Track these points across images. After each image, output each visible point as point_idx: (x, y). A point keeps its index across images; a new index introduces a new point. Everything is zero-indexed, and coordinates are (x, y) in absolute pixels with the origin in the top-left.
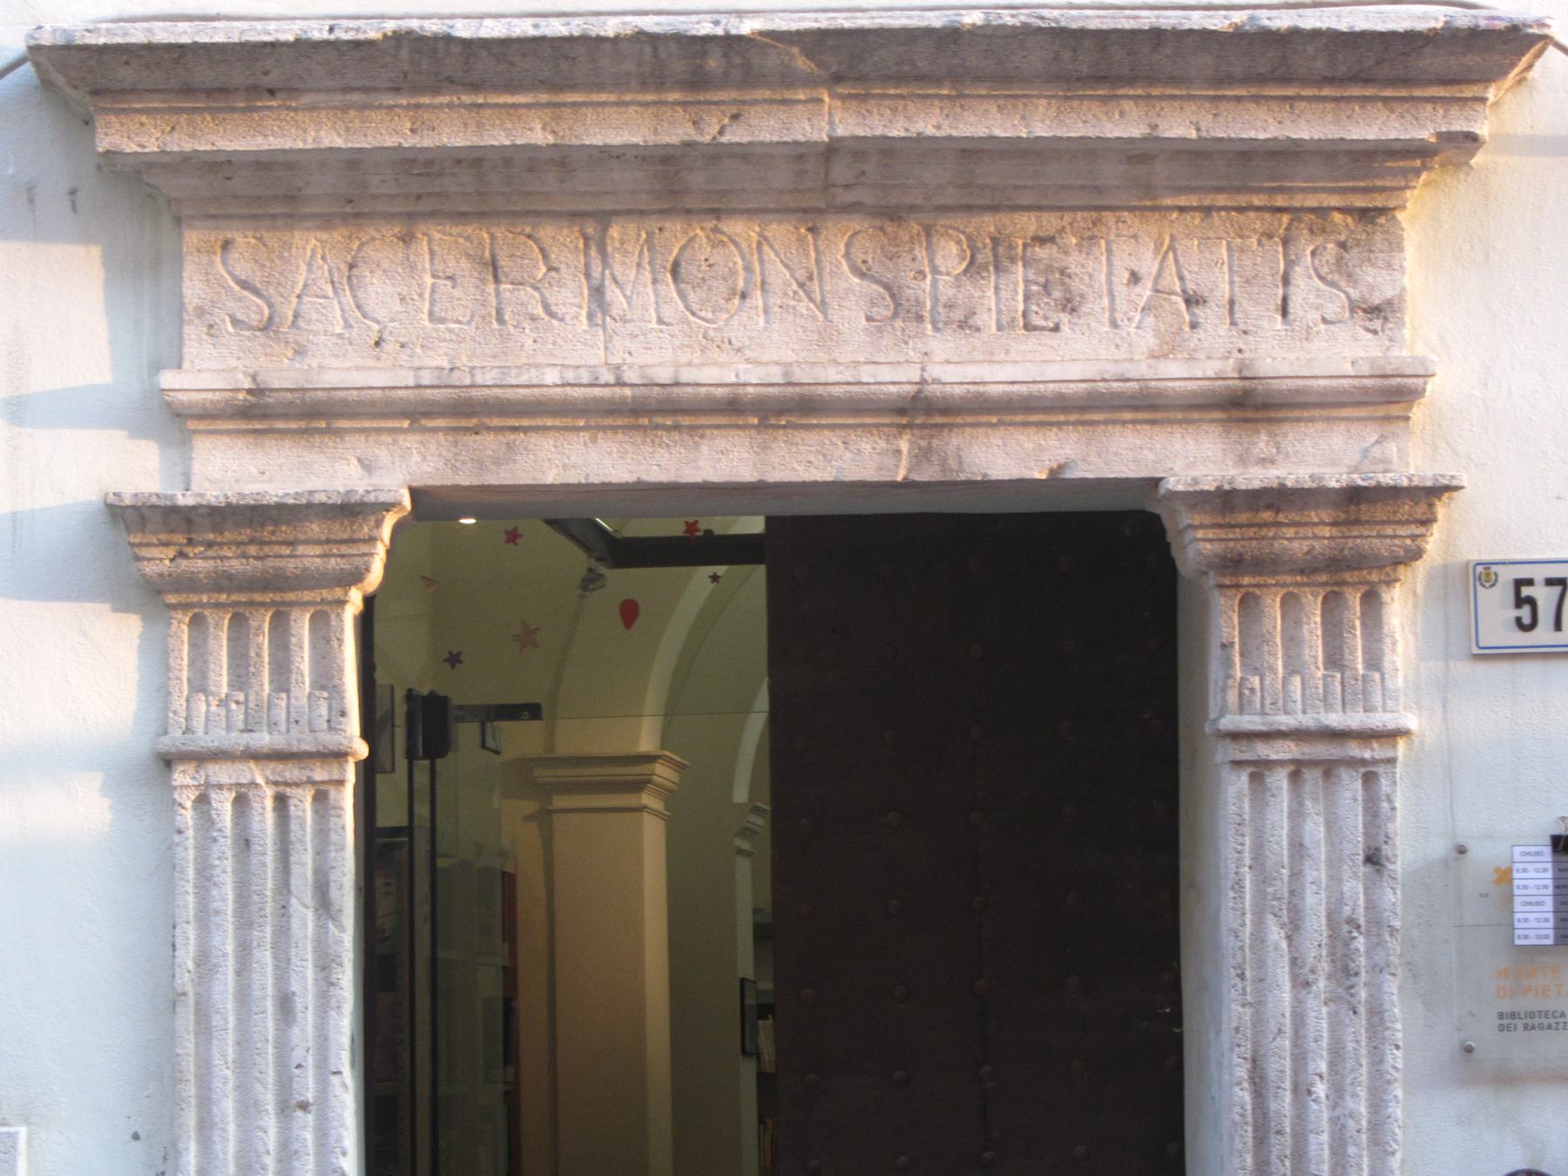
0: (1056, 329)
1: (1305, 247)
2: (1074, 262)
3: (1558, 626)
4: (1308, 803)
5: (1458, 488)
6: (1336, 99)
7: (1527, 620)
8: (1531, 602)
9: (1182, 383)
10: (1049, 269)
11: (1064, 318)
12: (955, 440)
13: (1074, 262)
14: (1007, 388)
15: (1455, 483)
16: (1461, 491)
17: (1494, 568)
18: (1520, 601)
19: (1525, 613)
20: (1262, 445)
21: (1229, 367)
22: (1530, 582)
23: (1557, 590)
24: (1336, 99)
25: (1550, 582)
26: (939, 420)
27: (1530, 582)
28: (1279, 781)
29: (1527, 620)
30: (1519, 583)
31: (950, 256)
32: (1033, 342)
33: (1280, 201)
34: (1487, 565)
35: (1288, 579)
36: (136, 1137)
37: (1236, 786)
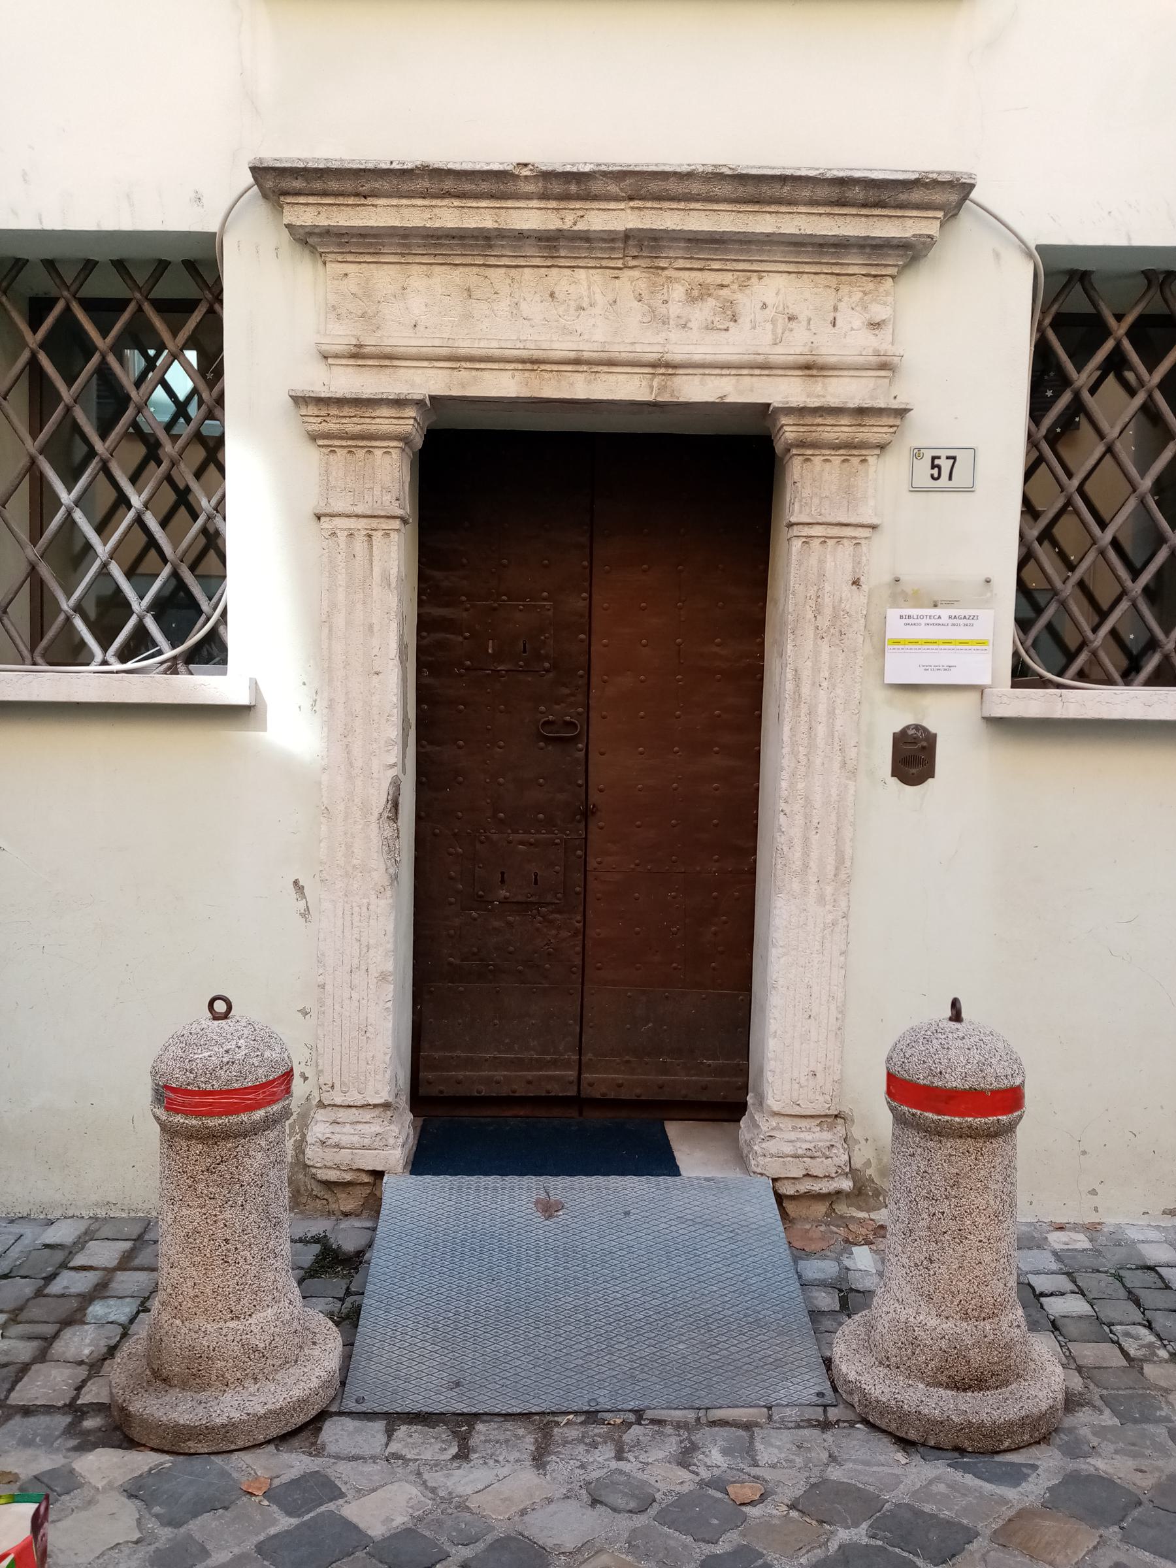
0: (727, 330)
1: (845, 289)
2: (739, 296)
3: (950, 478)
4: (828, 556)
5: (910, 410)
6: (867, 216)
7: (936, 475)
8: (939, 467)
9: (784, 357)
10: (726, 300)
11: (732, 324)
12: (677, 381)
13: (739, 296)
14: (704, 356)
15: (908, 407)
16: (911, 412)
17: (922, 451)
18: (933, 466)
19: (935, 472)
20: (656, 1454)
21: (806, 350)
22: (939, 458)
23: (952, 461)
24: (867, 216)
25: (948, 458)
26: (670, 371)
27: (939, 458)
28: (815, 543)
29: (936, 475)
30: (934, 458)
31: (678, 292)
32: (715, 336)
33: (837, 270)
34: (919, 450)
35: (827, 452)
36: (304, 684)
37: (797, 545)
